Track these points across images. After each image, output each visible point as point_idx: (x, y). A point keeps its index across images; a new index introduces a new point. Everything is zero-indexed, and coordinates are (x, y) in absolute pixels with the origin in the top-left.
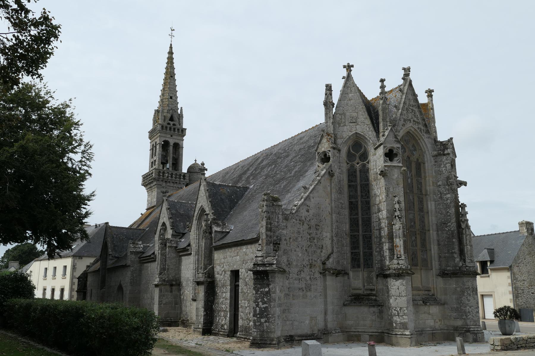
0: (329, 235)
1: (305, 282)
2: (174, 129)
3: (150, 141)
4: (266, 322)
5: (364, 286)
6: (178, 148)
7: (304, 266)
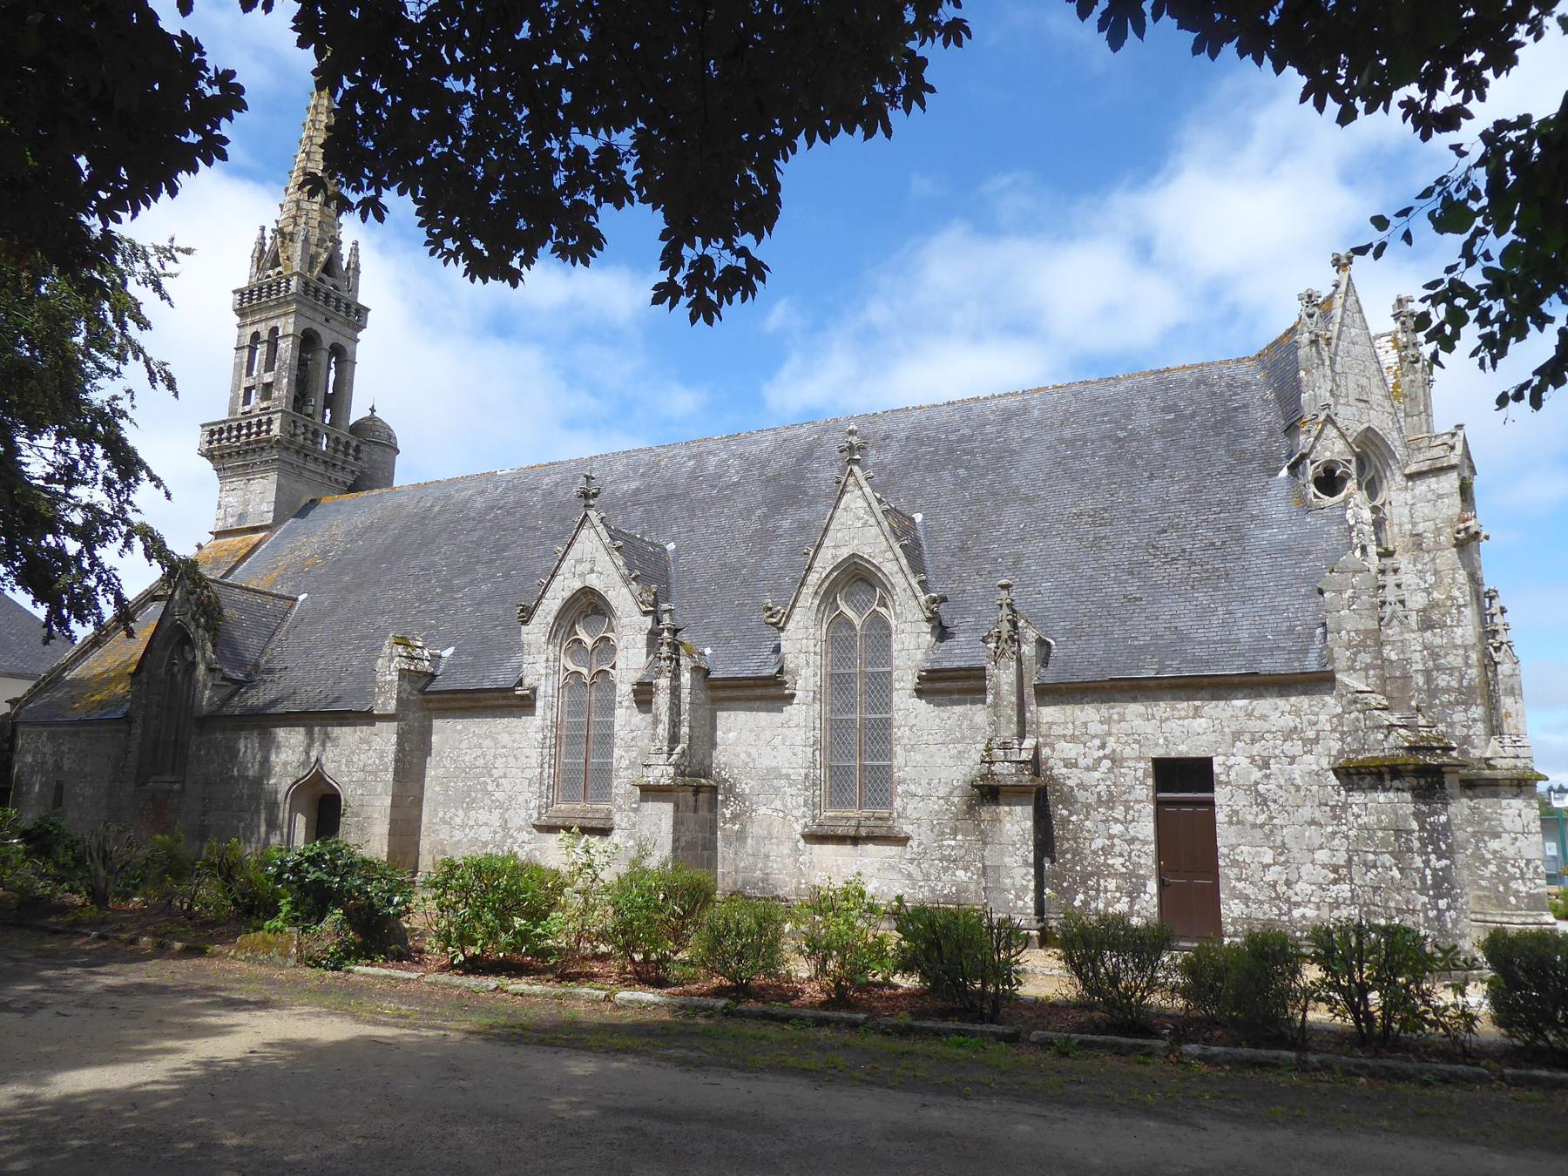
3: (237, 320)
4: (1449, 908)
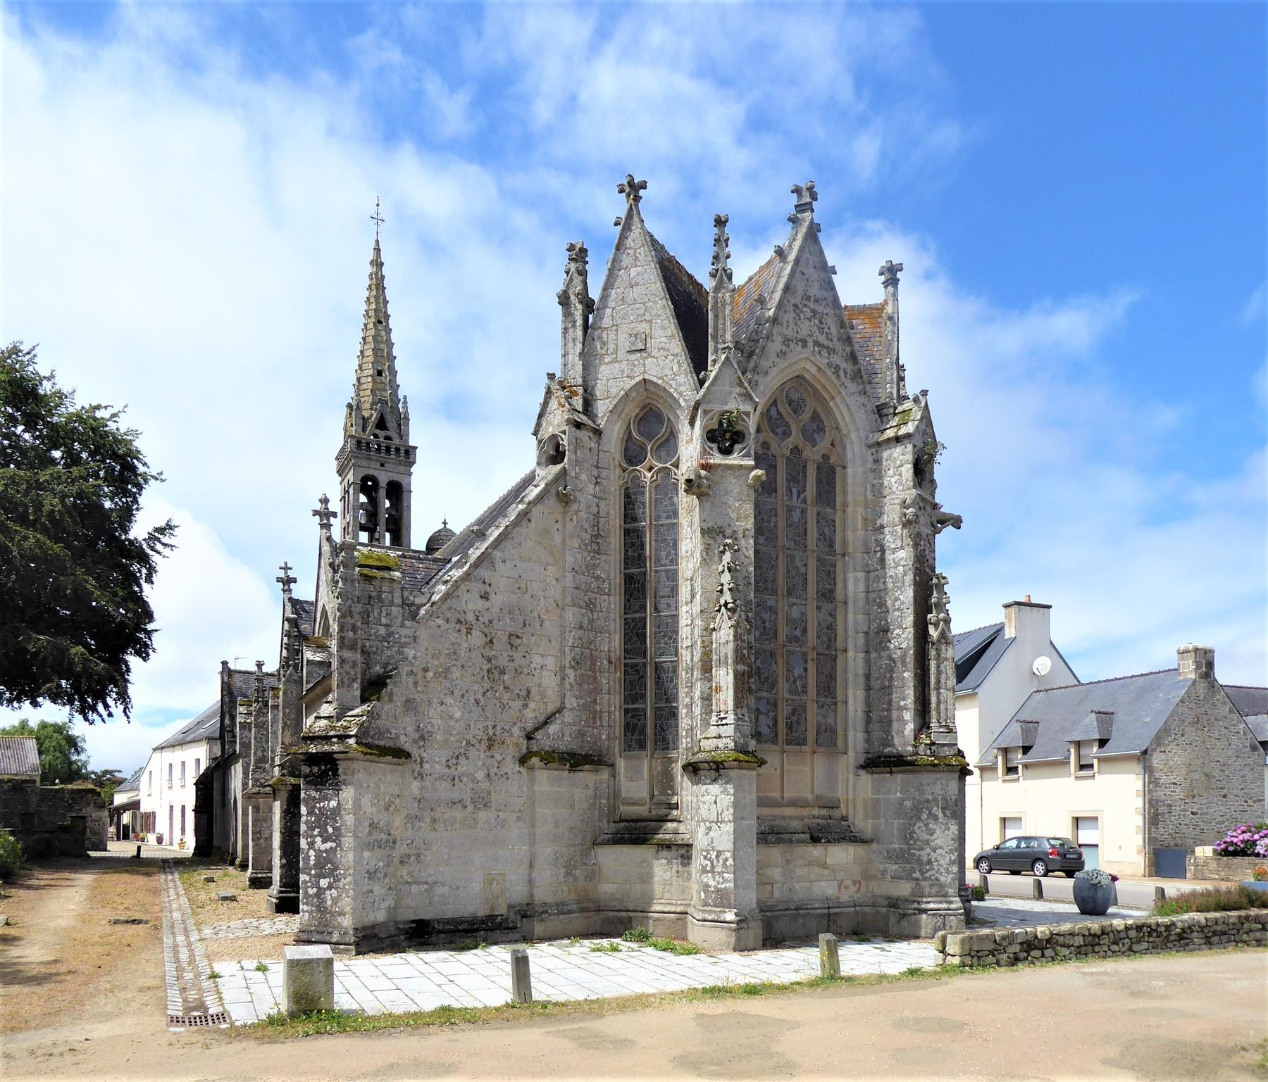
0: (551, 663)
1: (470, 785)
2: (388, 449)
4: (330, 887)
5: (652, 796)
6: (398, 492)
7: (468, 743)
